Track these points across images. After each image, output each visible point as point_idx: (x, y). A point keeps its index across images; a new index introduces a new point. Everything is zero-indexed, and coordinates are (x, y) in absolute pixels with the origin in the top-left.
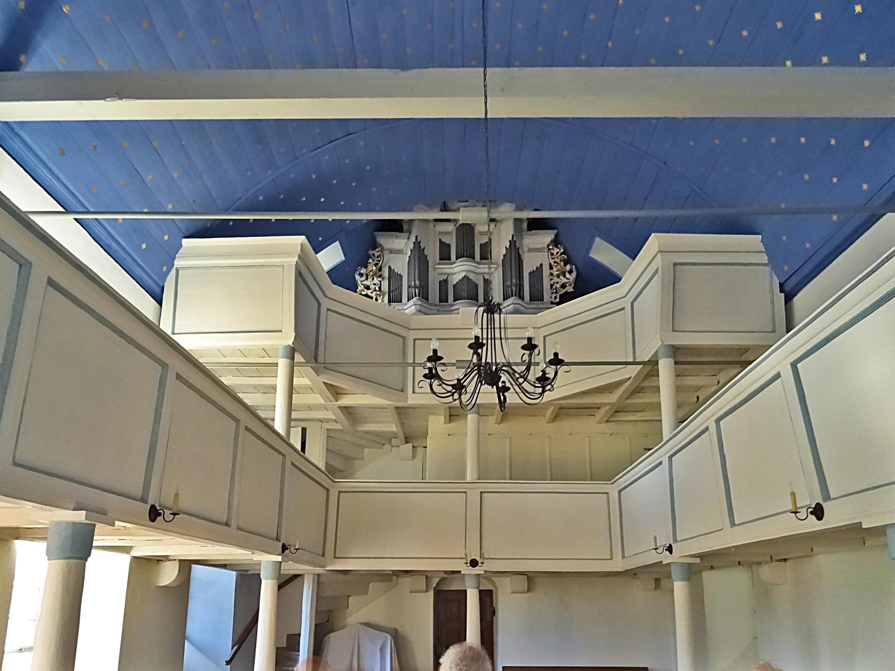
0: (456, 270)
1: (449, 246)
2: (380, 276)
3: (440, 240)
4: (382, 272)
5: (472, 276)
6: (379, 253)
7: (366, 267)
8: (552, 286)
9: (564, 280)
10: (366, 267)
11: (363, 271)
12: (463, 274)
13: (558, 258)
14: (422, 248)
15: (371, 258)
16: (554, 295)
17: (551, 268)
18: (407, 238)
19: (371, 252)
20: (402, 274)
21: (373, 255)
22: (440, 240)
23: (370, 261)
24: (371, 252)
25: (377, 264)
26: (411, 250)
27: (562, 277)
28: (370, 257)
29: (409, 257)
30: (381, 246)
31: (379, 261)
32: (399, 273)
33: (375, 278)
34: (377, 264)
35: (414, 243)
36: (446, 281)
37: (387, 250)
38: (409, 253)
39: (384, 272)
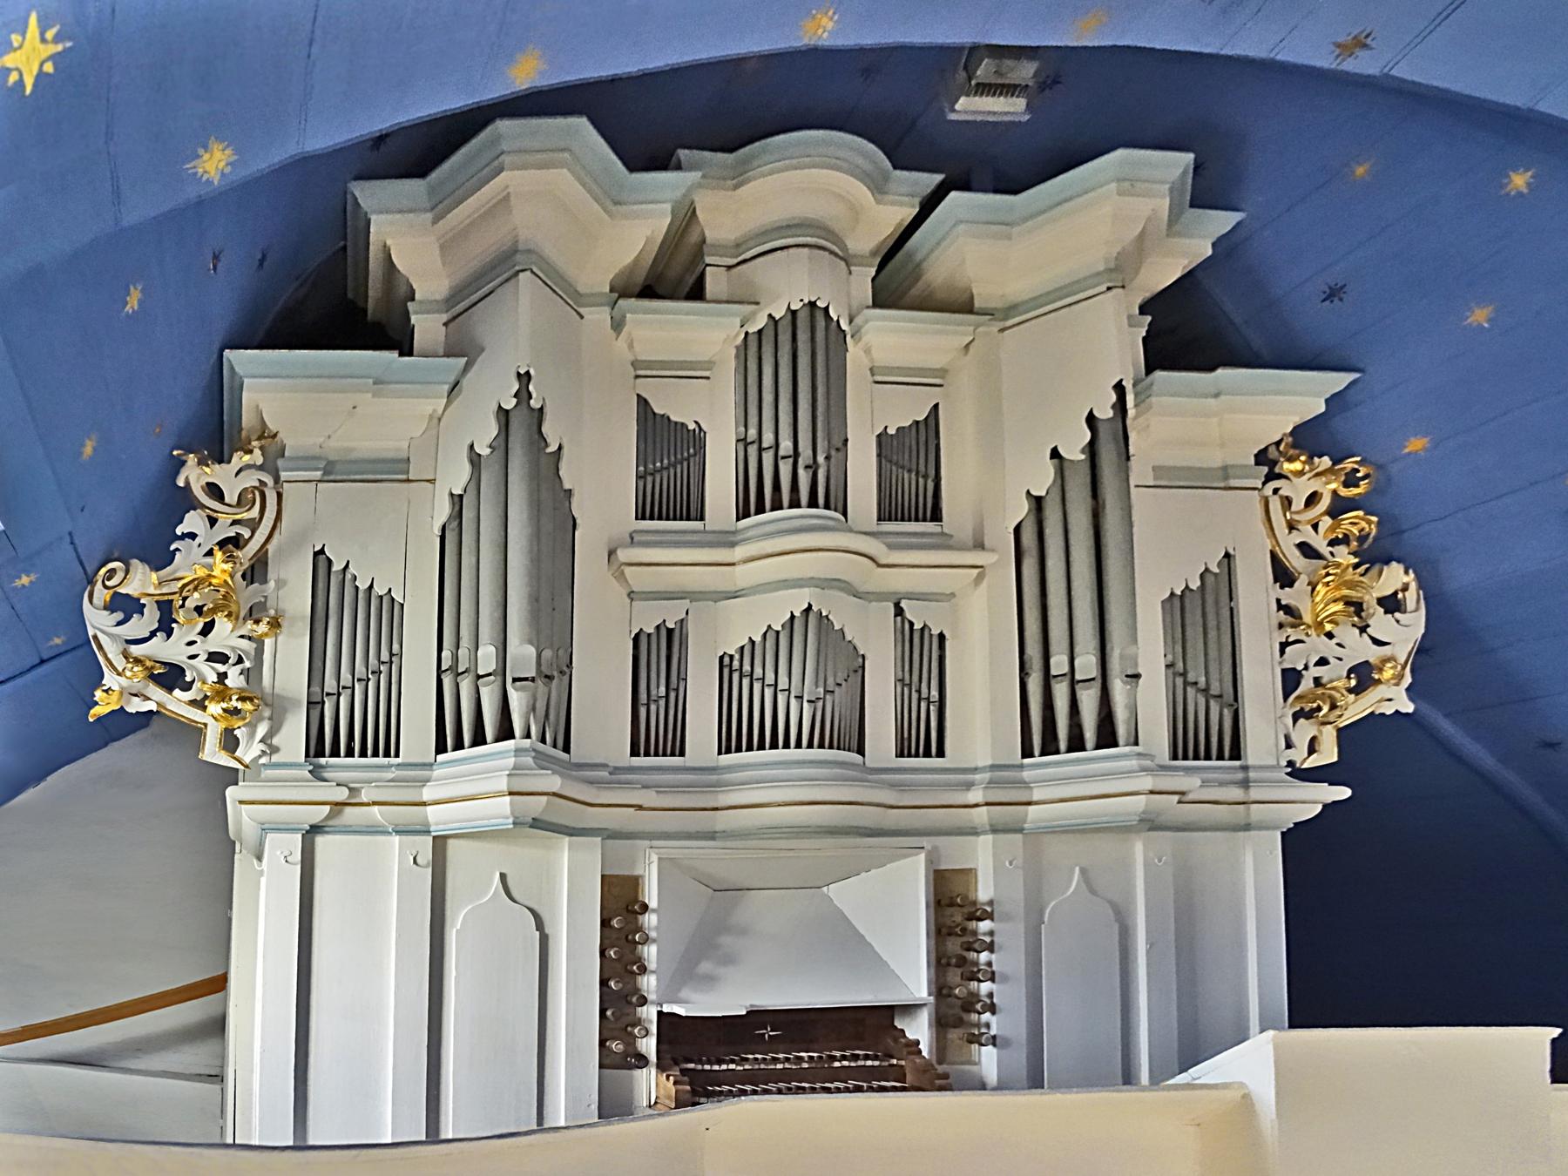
0: (744, 575)
1: (697, 440)
2: (254, 614)
3: (643, 402)
4: (272, 584)
5: (842, 612)
6: (250, 480)
7: (161, 559)
8: (1291, 679)
9: (1359, 649)
10: (161, 559)
11: (141, 581)
12: (797, 601)
13: (1315, 527)
14: (552, 448)
15: (195, 505)
16: (1306, 729)
17: (1284, 577)
18: (446, 387)
19: (194, 475)
20: (398, 598)
21: (215, 491)
22: (643, 402)
23: (192, 522)
24: (194, 475)
25: (236, 542)
26: (475, 460)
27: (1348, 634)
28: (187, 501)
29: (457, 500)
30: (265, 434)
31: (254, 525)
32: (379, 590)
33: (223, 625)
34: (236, 542)
35: (504, 415)
36: (672, 639)
37: (306, 461)
38: (457, 477)
39: (280, 584)
